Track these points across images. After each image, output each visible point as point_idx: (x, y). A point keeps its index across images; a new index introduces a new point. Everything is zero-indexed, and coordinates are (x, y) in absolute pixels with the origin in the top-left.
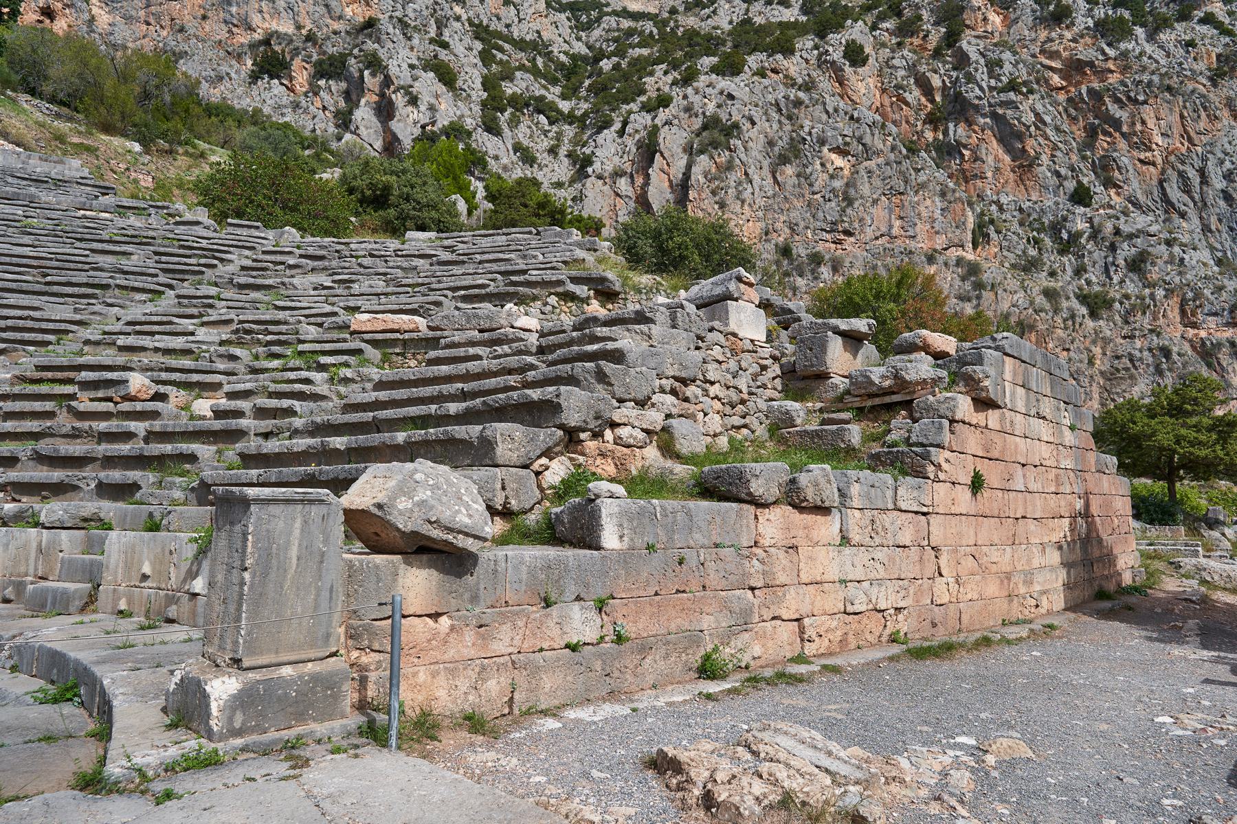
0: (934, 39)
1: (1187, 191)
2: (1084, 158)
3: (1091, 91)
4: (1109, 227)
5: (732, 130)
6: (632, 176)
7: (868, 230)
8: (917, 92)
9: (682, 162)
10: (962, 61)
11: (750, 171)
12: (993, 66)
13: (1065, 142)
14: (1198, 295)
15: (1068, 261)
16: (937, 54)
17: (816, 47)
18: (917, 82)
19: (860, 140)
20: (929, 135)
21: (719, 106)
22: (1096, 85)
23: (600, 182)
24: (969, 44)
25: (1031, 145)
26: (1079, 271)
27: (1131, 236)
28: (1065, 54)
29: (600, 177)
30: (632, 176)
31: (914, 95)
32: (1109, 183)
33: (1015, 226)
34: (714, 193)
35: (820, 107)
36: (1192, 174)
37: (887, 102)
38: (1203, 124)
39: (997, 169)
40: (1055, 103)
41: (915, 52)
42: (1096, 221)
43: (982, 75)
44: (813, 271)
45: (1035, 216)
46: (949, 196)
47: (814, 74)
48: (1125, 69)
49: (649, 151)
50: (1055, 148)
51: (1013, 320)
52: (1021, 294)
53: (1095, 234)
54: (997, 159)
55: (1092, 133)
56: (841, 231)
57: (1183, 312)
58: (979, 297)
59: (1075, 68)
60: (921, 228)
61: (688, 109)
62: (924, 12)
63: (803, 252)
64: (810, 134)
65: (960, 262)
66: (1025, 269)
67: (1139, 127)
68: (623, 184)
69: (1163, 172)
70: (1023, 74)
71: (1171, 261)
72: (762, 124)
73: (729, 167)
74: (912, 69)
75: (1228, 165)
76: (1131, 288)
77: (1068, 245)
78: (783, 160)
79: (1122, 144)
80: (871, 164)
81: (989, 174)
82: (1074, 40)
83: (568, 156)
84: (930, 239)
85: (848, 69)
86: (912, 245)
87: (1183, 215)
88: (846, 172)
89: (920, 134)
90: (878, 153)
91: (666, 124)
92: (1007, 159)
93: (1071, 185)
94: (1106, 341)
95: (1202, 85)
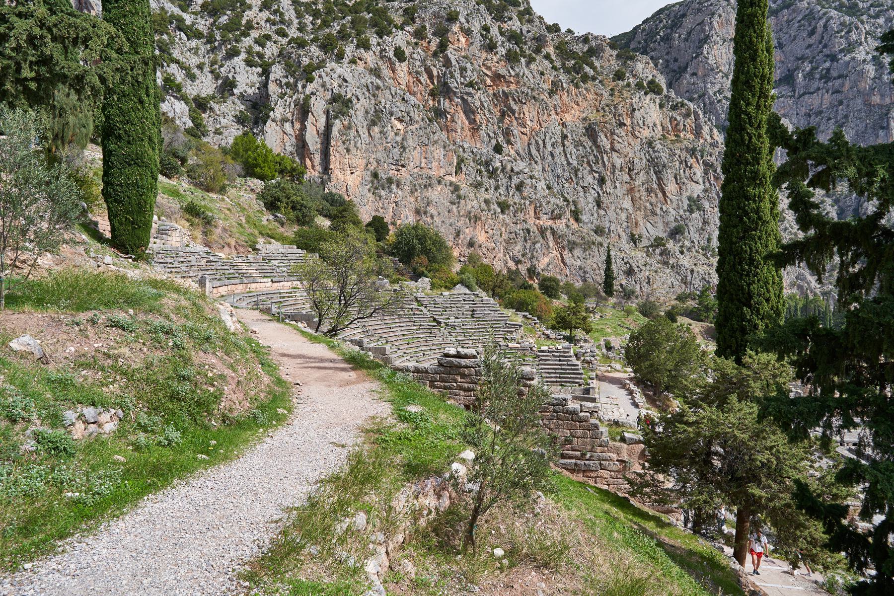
0: (433, 47)
1: (538, 151)
2: (499, 127)
3: (503, 92)
4: (509, 168)
5: (347, 104)
6: (292, 122)
7: (411, 164)
8: (425, 76)
9: (323, 120)
10: (447, 63)
11: (359, 129)
12: (463, 70)
13: (492, 118)
14: (541, 205)
15: (492, 181)
16: (435, 54)
17: (379, 44)
18: (425, 69)
19: (408, 114)
20: (431, 102)
21: (340, 86)
22: (505, 89)
23: (274, 124)
24: (450, 52)
25: (478, 117)
26: (497, 188)
27: (518, 173)
28: (493, 69)
29: (274, 121)
30: (292, 122)
31: (424, 78)
32: (509, 142)
33: (472, 164)
34: (344, 143)
35: (388, 91)
36: (541, 142)
37: (411, 80)
38: (545, 117)
39: (463, 128)
40: (488, 96)
41: (424, 51)
42: (504, 162)
43: (457, 75)
44: (389, 187)
45: (478, 157)
46: (447, 149)
47: (380, 64)
48: (518, 83)
49: (304, 110)
50: (488, 121)
51: (472, 214)
52: (475, 202)
53: (504, 169)
54: (463, 123)
55: (503, 114)
56: (400, 165)
57: (535, 212)
58: (459, 203)
59: (497, 77)
60: (434, 164)
61: (323, 86)
62: (427, 24)
63: (384, 177)
64: (385, 107)
65: (451, 184)
66: (476, 187)
67: (522, 116)
68: (287, 126)
69: (530, 140)
70: (475, 78)
71: (531, 187)
72: (362, 100)
73: (349, 127)
74: (423, 61)
75: (553, 140)
76: (517, 199)
77: (492, 174)
78: (373, 123)
79: (515, 123)
80: (413, 127)
81: (459, 130)
82: (497, 62)
83: (212, 72)
84: (438, 170)
85: (397, 64)
86: (431, 173)
87: (536, 162)
88: (402, 132)
89: (426, 101)
90: (416, 122)
91: (312, 93)
92: (467, 122)
93: (494, 142)
94: (507, 225)
95: (544, 97)
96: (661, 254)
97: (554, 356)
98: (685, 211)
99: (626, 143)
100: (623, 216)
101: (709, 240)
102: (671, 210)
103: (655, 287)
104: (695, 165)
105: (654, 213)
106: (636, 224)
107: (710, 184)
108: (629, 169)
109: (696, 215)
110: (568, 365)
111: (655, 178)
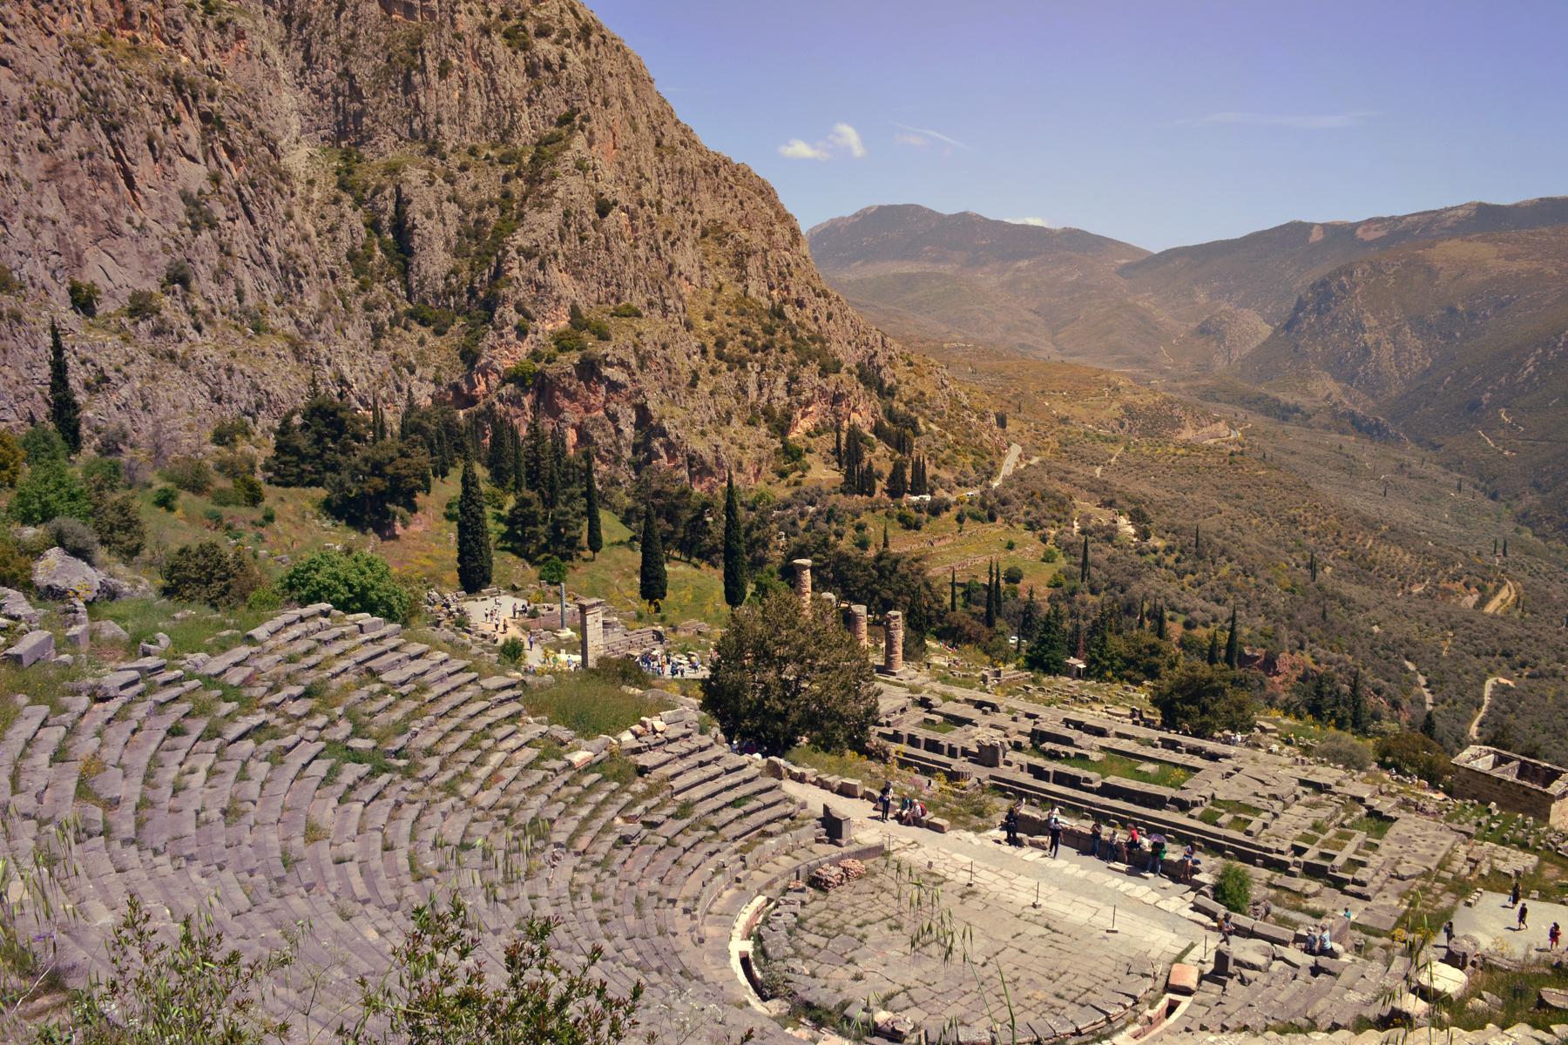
96: (157, 332)
97: (682, 756)
98: (181, 226)
99: (24, 44)
100: (47, 238)
101: (240, 294)
102: (150, 223)
103: (161, 415)
104: (185, 117)
105: (116, 233)
106: (79, 257)
107: (219, 163)
108: (44, 116)
109: (205, 236)
110: (728, 772)
111: (105, 141)
